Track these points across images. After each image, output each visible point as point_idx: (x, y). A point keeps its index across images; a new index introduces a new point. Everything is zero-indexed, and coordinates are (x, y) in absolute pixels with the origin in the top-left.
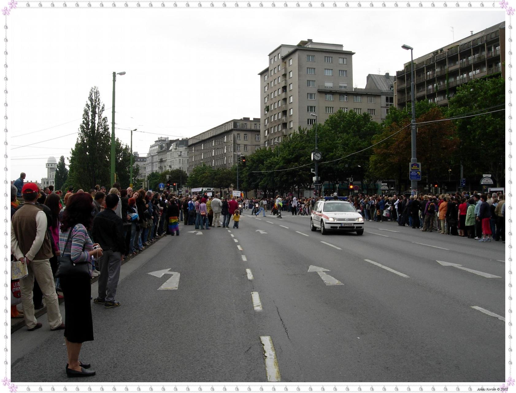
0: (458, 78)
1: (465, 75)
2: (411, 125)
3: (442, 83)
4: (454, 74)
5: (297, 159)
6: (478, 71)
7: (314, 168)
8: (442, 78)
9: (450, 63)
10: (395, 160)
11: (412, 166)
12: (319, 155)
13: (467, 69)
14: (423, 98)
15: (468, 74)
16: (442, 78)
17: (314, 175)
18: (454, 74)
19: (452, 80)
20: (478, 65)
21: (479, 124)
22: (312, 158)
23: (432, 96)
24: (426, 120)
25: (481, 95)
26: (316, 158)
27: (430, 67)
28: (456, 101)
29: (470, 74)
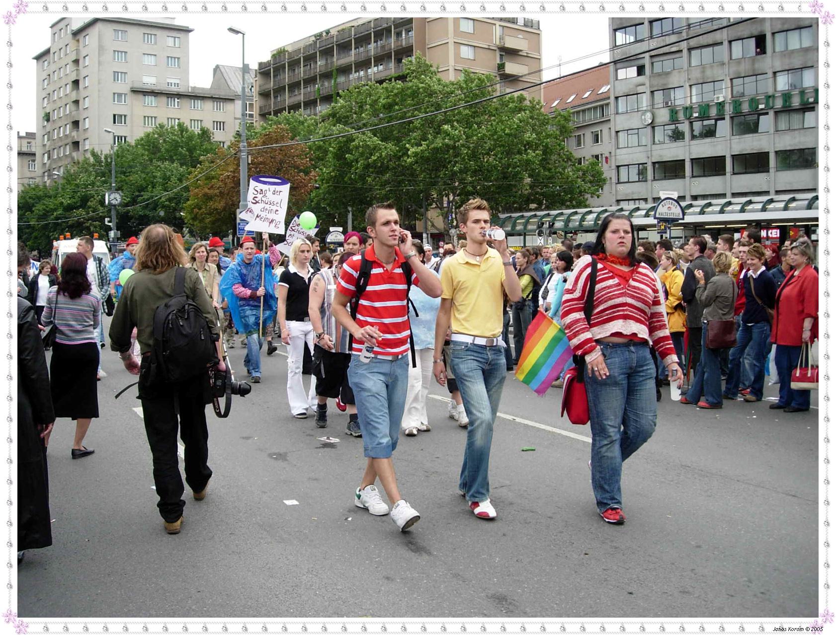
0: (351, 76)
1: (362, 73)
2: (240, 151)
3: (326, 84)
4: (345, 70)
5: (84, 202)
6: (381, 68)
7: (110, 217)
8: (327, 76)
9: (339, 53)
10: (219, 205)
13: (364, 64)
14: (295, 107)
15: (367, 71)
16: (327, 76)
17: (110, 229)
18: (345, 70)
19: (341, 79)
20: (380, 59)
22: (107, 202)
23: (310, 104)
24: (264, 143)
26: (114, 202)
27: (310, 59)
29: (369, 70)
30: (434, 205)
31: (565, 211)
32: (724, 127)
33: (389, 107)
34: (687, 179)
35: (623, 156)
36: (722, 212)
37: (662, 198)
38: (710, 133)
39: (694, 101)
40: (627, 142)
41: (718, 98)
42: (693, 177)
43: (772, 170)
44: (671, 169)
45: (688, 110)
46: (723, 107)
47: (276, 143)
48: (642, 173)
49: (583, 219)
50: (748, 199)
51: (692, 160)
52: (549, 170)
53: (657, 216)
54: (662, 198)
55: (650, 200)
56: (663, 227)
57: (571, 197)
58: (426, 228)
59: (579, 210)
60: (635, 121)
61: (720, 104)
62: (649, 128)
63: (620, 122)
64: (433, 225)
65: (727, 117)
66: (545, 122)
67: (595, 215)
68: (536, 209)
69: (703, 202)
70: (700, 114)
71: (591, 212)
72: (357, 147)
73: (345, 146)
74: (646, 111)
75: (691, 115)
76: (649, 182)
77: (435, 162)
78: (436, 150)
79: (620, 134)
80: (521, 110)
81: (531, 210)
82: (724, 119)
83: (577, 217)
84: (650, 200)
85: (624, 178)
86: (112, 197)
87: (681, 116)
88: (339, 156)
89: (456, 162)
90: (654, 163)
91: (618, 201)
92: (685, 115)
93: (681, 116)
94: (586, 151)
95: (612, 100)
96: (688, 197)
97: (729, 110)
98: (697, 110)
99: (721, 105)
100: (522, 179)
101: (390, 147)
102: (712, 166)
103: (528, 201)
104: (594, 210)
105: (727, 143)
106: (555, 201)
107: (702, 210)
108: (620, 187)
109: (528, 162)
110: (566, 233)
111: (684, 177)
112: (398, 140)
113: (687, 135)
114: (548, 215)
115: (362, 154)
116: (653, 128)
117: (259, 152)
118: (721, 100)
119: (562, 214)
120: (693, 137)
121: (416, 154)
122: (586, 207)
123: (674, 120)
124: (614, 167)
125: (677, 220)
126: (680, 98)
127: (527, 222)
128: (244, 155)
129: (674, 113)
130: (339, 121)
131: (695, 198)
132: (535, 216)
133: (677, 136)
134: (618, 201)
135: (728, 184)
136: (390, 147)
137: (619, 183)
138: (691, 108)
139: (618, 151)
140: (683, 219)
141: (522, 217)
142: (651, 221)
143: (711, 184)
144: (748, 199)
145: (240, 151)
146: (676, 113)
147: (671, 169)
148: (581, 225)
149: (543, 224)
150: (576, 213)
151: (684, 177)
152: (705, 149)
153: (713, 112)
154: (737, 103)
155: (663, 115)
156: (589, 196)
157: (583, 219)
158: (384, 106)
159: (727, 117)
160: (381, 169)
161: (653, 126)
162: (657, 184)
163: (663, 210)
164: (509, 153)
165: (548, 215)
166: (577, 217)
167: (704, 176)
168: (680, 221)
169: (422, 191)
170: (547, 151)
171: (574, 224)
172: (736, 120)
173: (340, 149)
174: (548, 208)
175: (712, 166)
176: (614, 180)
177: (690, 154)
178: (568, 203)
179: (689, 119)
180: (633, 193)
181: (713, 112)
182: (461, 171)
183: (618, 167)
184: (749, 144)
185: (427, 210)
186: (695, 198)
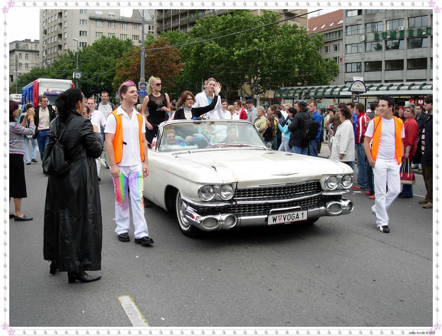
11: (141, 85)
12: (79, 74)
14: (175, 28)
21: (208, 51)
25: (213, 29)
26: (77, 77)
28: (192, 33)
30: (247, 82)
31: (315, 87)
32: (404, 44)
33: (224, 29)
34: (383, 71)
35: (349, 59)
36: (378, 90)
38: (396, 47)
39: (388, 29)
40: (351, 51)
41: (401, 28)
42: (386, 70)
45: (384, 34)
46: (404, 33)
47: (162, 46)
48: (359, 67)
50: (412, 83)
52: (309, 64)
53: (351, 90)
56: (354, 96)
57: (319, 79)
58: (242, 94)
59: (323, 87)
60: (356, 41)
61: (402, 31)
62: (363, 43)
63: (348, 39)
64: (245, 93)
65: (405, 39)
66: (308, 40)
67: (331, 89)
68: (301, 86)
70: (391, 36)
71: (329, 88)
72: (206, 50)
73: (200, 49)
74: (362, 34)
75: (386, 37)
76: (363, 72)
77: (248, 59)
78: (248, 53)
79: (348, 46)
80: (294, 32)
81: (298, 86)
82: (403, 39)
86: (77, 74)
87: (381, 38)
88: (197, 54)
89: (259, 60)
90: (365, 63)
91: (346, 82)
92: (383, 37)
93: (381, 38)
95: (344, 28)
97: (406, 34)
98: (390, 34)
99: (402, 32)
100: (294, 69)
101: (224, 51)
102: (396, 65)
103: (297, 80)
104: (330, 86)
106: (311, 82)
107: (387, 88)
108: (347, 75)
109: (297, 62)
110: (315, 98)
111: (381, 70)
112: (228, 47)
113: (384, 48)
114: (306, 89)
115: (209, 54)
116: (366, 43)
117: (152, 52)
118: (402, 29)
119: (313, 88)
120: (387, 48)
122: (327, 85)
123: (377, 39)
124: (344, 63)
125: (362, 92)
126: (381, 28)
127: (295, 93)
128: (143, 53)
129: (377, 35)
130: (197, 36)
131: (386, 81)
133: (379, 48)
134: (346, 82)
135: (405, 74)
136: (224, 51)
137: (346, 72)
138: (386, 33)
139: (346, 55)
141: (293, 89)
143: (396, 74)
144: (412, 83)
145: (140, 51)
146: (378, 36)
147: (375, 66)
148: (323, 94)
149: (301, 93)
150: (321, 88)
151: (381, 70)
152: (393, 55)
153: (398, 36)
154: (411, 31)
155: (371, 37)
157: (324, 91)
158: (221, 29)
159: (405, 39)
160: (218, 61)
161: (365, 42)
162: (367, 74)
163: (355, 87)
164: (287, 56)
165: (306, 89)
166: (321, 90)
168: (364, 94)
169: (239, 74)
170: (308, 55)
171: (319, 94)
172: (410, 40)
173: (198, 50)
175: (396, 65)
176: (344, 71)
177: (385, 58)
179: (385, 39)
181: (398, 36)
183: (346, 64)
185: (243, 84)
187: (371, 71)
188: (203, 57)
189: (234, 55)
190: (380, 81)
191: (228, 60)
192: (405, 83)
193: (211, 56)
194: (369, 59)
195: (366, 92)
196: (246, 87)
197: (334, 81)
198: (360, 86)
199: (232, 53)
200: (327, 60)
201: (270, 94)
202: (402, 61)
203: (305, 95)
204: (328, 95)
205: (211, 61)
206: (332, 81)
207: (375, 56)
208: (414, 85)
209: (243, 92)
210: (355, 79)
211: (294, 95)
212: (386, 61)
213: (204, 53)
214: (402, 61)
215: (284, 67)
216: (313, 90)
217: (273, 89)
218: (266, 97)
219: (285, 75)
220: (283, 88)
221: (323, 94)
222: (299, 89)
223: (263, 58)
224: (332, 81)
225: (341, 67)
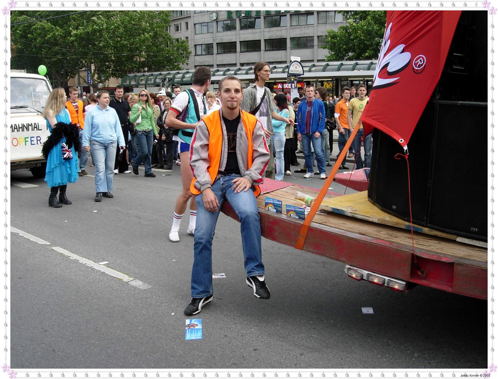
30: (84, 69)
31: (171, 72)
34: (238, 54)
37: (292, 61)
42: (241, 52)
43: (288, 49)
44: (228, 47)
49: (184, 77)
51: (265, 40)
54: (292, 61)
55: (215, 66)
56: (292, 79)
64: (85, 81)
68: (148, 71)
69: (247, 67)
76: (215, 55)
81: (145, 72)
83: (181, 75)
84: (215, 66)
85: (199, 52)
89: (101, 41)
90: (217, 44)
94: (181, 35)
96: (238, 65)
101: (59, 31)
102: (253, 46)
105: (261, 33)
108: (197, 58)
111: (235, 52)
115: (39, 35)
121: (76, 35)
124: (193, 46)
125: (300, 75)
131: (242, 65)
132: (152, 75)
135: (262, 57)
136: (59, 31)
137: (196, 55)
139: (196, 36)
140: (303, 74)
142: (285, 75)
147: (228, 47)
148: (182, 80)
149: (165, 79)
150: (179, 73)
151: (235, 52)
156: (181, 64)
157: (184, 77)
165: (161, 74)
167: (248, 51)
168: (302, 76)
170: (156, 34)
174: (158, 71)
175: (253, 46)
177: (240, 38)
178: (168, 67)
180: (205, 62)
182: (104, 46)
183: (195, 46)
184: (275, 33)
186: (242, 65)
187: (224, 52)
188: (32, 39)
189: (71, 36)
190: (235, 65)
191: (63, 42)
192: (317, 64)
193: (42, 37)
194: (222, 39)
195: (303, 74)
196: (83, 74)
197: (187, 64)
198: (298, 67)
199: (69, 34)
200: (177, 40)
201: (113, 82)
202: (259, 41)
203: (169, 81)
204: (188, 81)
205: (43, 43)
206: (185, 64)
207: (228, 37)
208: (275, 68)
209: (81, 80)
210: (293, 59)
211: (146, 82)
212: (240, 42)
213: (33, 34)
214: (259, 41)
215: (131, 50)
216: (157, 76)
217: (114, 75)
218: (106, 86)
219: (130, 58)
220: (131, 75)
221: (182, 80)
222: (152, 75)
223: (106, 39)
224: (185, 64)
225: (191, 49)
